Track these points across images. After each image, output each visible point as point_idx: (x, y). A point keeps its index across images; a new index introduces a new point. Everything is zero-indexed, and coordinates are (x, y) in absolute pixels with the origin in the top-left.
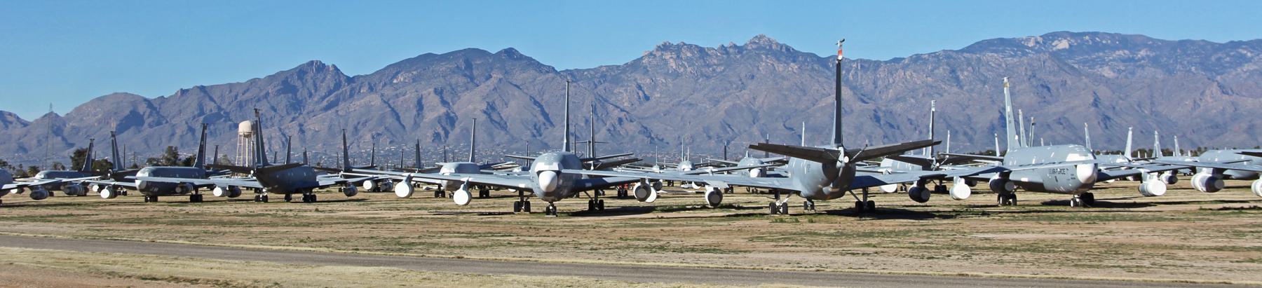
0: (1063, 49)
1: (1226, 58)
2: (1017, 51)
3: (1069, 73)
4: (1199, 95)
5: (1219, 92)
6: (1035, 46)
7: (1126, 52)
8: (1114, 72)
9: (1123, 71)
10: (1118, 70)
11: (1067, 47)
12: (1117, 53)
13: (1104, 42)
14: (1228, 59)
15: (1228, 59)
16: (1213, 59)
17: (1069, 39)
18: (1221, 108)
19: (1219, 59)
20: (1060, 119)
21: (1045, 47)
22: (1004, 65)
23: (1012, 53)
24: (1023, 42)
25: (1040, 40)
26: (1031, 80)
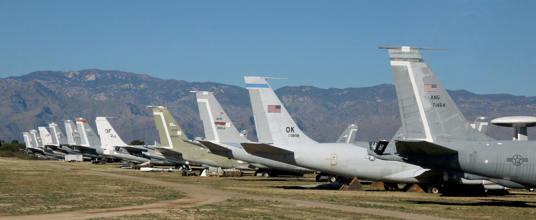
0: (91, 80)
1: (181, 92)
2: (58, 80)
3: (43, 95)
4: (119, 114)
5: (130, 112)
6: (72, 78)
7: (131, 85)
8: (106, 97)
9: (113, 97)
10: (109, 96)
11: (94, 79)
12: (125, 85)
13: (119, 78)
14: (183, 93)
15: (183, 93)
16: (174, 92)
17: (97, 74)
18: (123, 122)
19: (177, 93)
20: (10, 124)
21: (79, 79)
22: (6, 88)
23: (54, 81)
24: (65, 74)
25: (77, 73)
26: (13, 98)
